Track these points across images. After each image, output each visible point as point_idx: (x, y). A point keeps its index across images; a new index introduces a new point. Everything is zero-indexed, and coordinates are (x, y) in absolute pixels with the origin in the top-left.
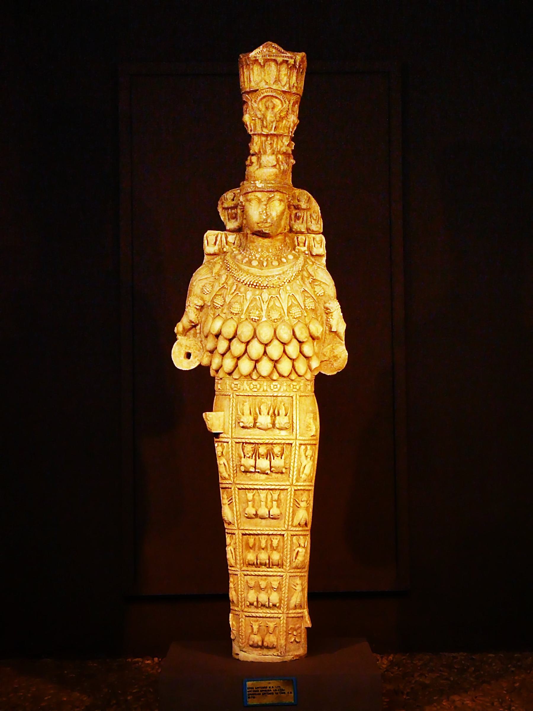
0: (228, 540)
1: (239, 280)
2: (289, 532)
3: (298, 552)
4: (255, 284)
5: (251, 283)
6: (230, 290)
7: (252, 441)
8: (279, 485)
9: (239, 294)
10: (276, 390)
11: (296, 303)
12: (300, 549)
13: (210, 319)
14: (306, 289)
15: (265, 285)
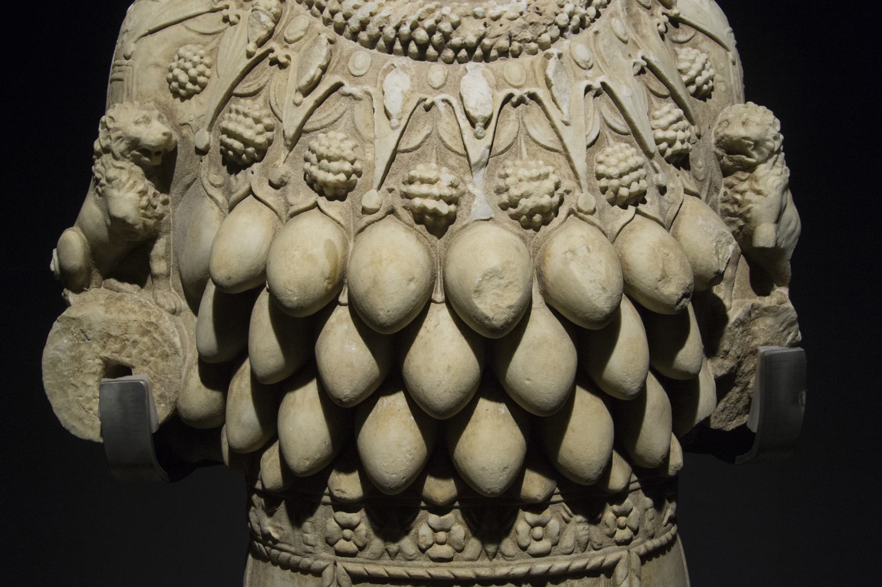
1: (339, 18)
4: (421, 35)
5: (405, 30)
6: (302, 69)
9: (347, 88)
10: (544, 545)
11: (620, 124)
13: (211, 213)
14: (653, 59)
15: (472, 39)
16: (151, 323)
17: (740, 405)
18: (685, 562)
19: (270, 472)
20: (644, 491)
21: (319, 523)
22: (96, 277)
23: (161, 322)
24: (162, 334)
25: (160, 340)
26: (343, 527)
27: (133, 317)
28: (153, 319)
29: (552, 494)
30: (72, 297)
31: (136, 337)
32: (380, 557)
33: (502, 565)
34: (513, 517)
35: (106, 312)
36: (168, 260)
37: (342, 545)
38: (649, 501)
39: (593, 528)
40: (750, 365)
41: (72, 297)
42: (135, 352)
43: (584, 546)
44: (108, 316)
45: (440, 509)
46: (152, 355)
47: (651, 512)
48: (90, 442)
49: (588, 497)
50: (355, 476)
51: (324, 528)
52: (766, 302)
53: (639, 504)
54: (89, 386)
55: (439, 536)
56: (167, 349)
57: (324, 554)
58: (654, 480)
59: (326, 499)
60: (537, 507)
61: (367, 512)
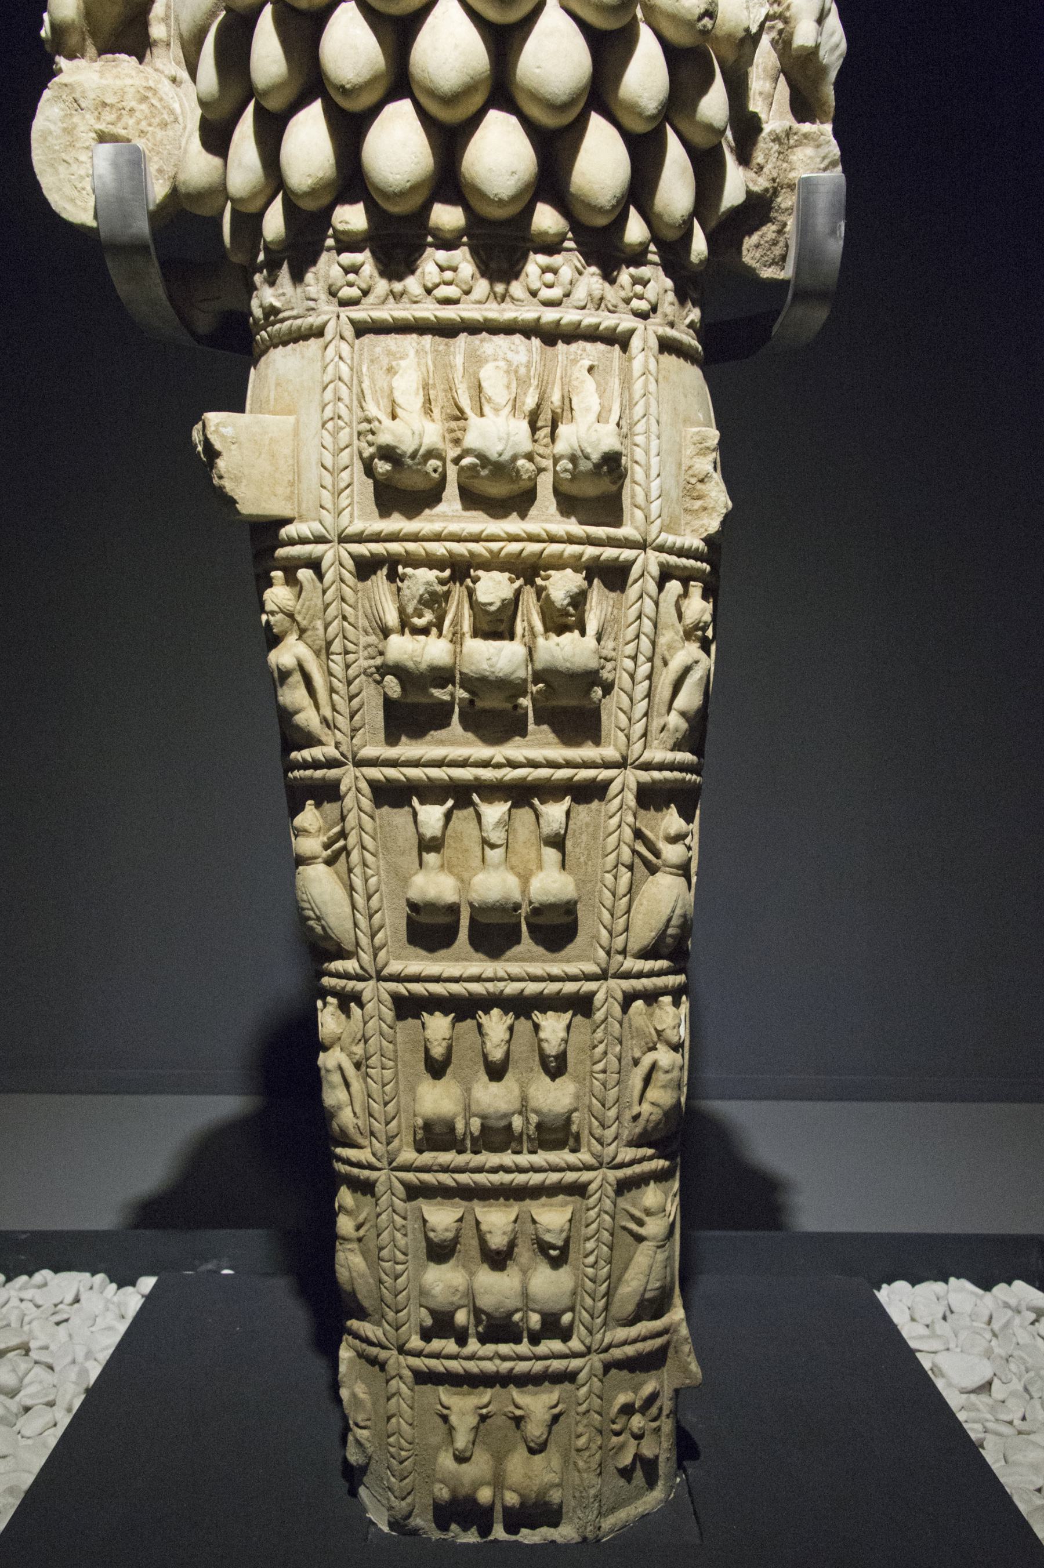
0: (329, 1020)
2: (613, 983)
3: (654, 1067)
7: (439, 549)
8: (569, 764)
10: (555, 293)
12: (664, 1057)
16: (151, 88)
17: (778, 251)
18: (712, 414)
19: (274, 223)
20: (664, 270)
21: (322, 273)
22: (91, 50)
23: (160, 86)
24: (161, 100)
25: (159, 106)
26: (347, 270)
27: (129, 81)
28: (151, 84)
29: (563, 238)
30: (62, 62)
31: (133, 104)
32: (384, 302)
33: (510, 309)
34: (524, 258)
35: (101, 78)
36: (168, 26)
37: (346, 292)
38: (669, 283)
39: (607, 285)
40: (786, 200)
41: (62, 62)
42: (131, 122)
43: (600, 303)
44: (104, 82)
45: (448, 243)
46: (150, 125)
47: (671, 296)
48: (83, 227)
49: (604, 249)
50: (360, 207)
51: (327, 276)
52: (806, 127)
53: (659, 284)
54: (82, 162)
55: (447, 273)
56: (166, 116)
57: (326, 308)
58: (671, 249)
59: (330, 242)
60: (551, 247)
61: (373, 252)
